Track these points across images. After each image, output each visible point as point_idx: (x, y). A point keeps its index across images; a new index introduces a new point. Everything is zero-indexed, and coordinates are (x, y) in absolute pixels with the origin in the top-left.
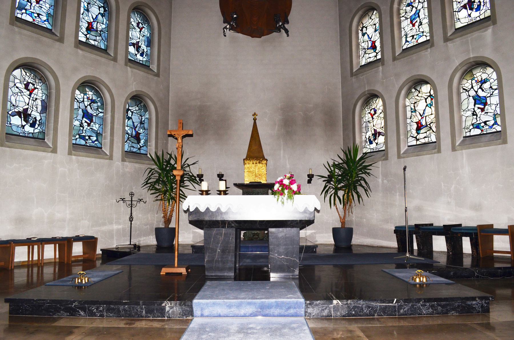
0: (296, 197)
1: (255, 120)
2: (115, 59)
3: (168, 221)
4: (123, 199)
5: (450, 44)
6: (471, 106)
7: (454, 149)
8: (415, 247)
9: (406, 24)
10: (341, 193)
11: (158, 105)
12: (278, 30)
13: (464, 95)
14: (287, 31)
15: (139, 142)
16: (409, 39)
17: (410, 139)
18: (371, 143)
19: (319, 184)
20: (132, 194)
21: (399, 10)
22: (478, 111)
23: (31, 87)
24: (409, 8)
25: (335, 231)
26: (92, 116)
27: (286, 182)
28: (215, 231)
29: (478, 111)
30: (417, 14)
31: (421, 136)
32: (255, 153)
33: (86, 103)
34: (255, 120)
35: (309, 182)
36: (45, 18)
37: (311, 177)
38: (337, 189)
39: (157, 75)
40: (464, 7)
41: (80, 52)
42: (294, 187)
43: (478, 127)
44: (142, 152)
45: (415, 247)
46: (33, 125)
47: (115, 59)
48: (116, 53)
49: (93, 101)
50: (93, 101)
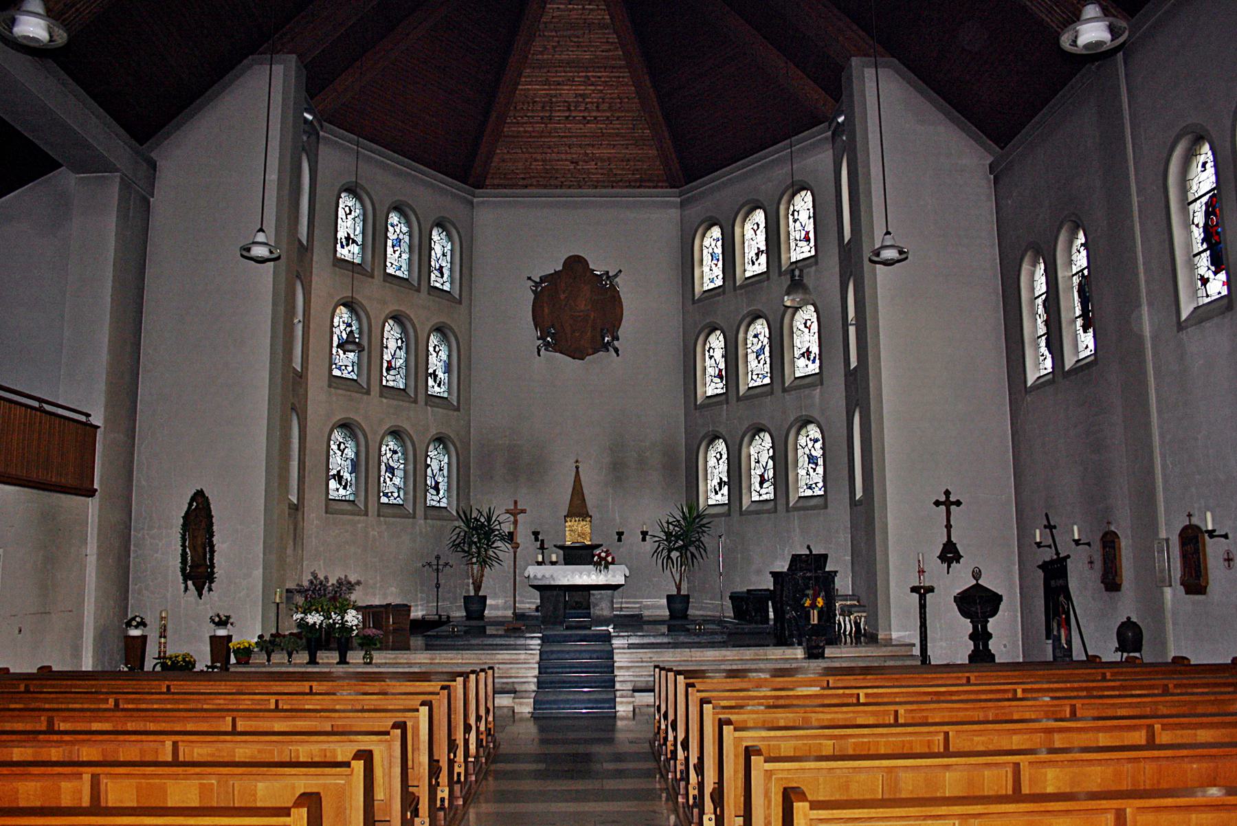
0: (611, 567)
1: (577, 468)
2: (415, 402)
3: (478, 588)
4: (429, 564)
5: (787, 397)
6: (806, 465)
7: (787, 511)
8: (771, 615)
9: (751, 357)
10: (675, 554)
11: (458, 445)
12: (606, 347)
13: (800, 452)
14: (616, 351)
15: (438, 493)
16: (755, 377)
17: (754, 493)
18: (716, 493)
19: (649, 546)
20: (438, 558)
21: (746, 339)
22: (811, 471)
23: (342, 446)
24: (755, 340)
25: (670, 598)
26: (393, 469)
27: (603, 555)
28: (548, 593)
29: (811, 471)
30: (763, 348)
31: (763, 491)
32: (578, 509)
33: (389, 455)
34: (577, 468)
35: (644, 539)
36: (350, 369)
37: (644, 534)
38: (670, 551)
39: (458, 409)
40: (803, 355)
41: (384, 400)
42: (610, 559)
43: (810, 488)
44: (442, 505)
45: (771, 615)
46: (345, 488)
47: (415, 402)
48: (416, 395)
49: (395, 452)
50: (395, 452)
